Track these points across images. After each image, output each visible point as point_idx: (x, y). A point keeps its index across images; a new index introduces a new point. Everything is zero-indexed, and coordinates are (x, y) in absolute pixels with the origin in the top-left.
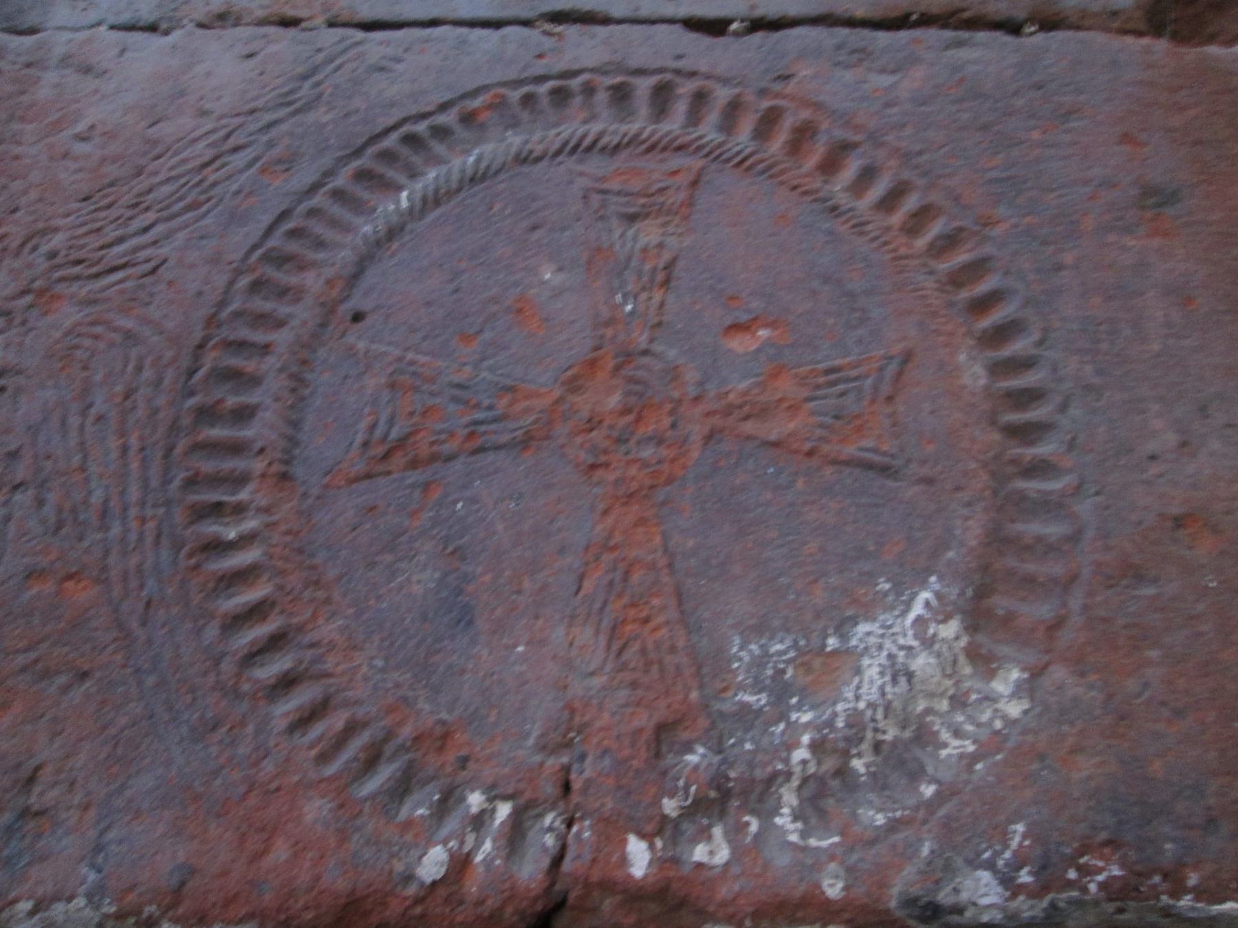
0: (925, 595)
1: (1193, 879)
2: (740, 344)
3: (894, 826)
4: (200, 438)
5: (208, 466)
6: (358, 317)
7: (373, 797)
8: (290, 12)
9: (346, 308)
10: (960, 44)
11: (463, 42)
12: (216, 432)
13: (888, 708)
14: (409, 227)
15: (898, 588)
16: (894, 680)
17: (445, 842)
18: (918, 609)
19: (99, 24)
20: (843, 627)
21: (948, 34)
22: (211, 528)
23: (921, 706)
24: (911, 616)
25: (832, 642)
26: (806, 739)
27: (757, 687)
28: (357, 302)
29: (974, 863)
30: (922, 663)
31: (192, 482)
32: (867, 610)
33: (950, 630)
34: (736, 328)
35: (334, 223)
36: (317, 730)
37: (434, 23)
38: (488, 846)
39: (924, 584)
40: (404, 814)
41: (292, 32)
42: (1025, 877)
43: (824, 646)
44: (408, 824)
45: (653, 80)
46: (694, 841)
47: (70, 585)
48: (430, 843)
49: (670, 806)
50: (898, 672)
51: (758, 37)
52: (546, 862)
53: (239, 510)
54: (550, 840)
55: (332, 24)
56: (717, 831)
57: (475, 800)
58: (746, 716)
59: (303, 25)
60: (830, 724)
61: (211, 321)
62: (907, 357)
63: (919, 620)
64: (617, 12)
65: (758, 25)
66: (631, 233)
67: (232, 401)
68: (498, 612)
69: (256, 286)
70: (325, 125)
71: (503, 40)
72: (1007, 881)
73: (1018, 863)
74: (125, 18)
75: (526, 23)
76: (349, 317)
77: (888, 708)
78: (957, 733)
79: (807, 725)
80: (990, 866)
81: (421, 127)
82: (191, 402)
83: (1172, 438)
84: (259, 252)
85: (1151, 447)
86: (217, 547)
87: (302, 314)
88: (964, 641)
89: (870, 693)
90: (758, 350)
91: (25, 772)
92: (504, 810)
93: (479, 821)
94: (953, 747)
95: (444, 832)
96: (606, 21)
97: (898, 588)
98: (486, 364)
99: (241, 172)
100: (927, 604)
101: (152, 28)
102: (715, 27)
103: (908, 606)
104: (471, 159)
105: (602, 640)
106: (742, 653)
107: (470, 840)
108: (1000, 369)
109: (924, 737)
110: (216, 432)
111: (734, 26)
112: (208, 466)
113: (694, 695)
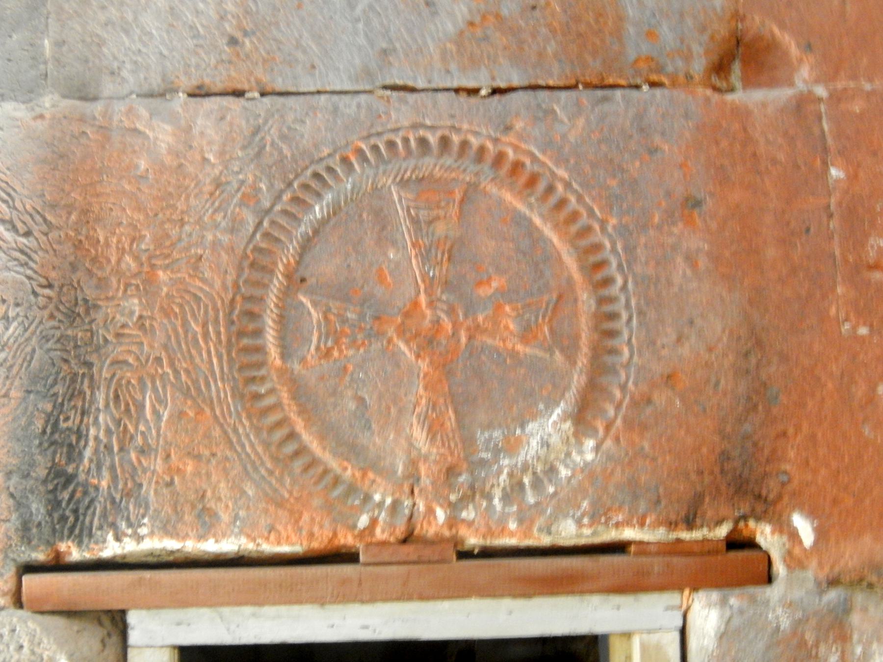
0: (558, 411)
1: (648, 521)
2: (484, 292)
3: (537, 504)
4: (241, 346)
5: (247, 359)
6: (303, 280)
7: (338, 497)
8: (239, 86)
9: (297, 277)
10: (605, 99)
11: (336, 109)
12: (245, 341)
13: (539, 458)
14: (321, 230)
15: (547, 407)
16: (542, 447)
17: (368, 513)
18: (554, 417)
19: (131, 93)
20: (523, 426)
21: (600, 93)
22: (254, 388)
23: (552, 456)
24: (551, 421)
25: (518, 432)
26: (505, 471)
27: (487, 450)
28: (302, 272)
29: (566, 516)
30: (555, 440)
31: (241, 369)
32: (534, 417)
33: (568, 425)
34: (479, 284)
35: (282, 228)
36: (312, 472)
37: (319, 92)
38: (383, 514)
39: (558, 405)
40: (349, 502)
41: (241, 101)
42: (586, 521)
43: (515, 433)
44: (352, 507)
45: (439, 134)
46: (461, 510)
47: (198, 417)
48: (361, 514)
49: (453, 498)
50: (545, 444)
51: (497, 97)
52: (405, 519)
53: (263, 379)
54: (407, 512)
55: (263, 94)
56: (471, 507)
57: (377, 497)
58: (483, 463)
59: (248, 95)
60: (516, 465)
61: (236, 285)
62: (560, 297)
63: (555, 423)
64: (421, 84)
65: (496, 91)
66: (431, 229)
67: (251, 327)
68: (381, 422)
69: (252, 265)
70: (270, 167)
71: (359, 106)
72: (579, 523)
73: (583, 515)
74: (146, 88)
75: (370, 92)
76: (299, 280)
77: (539, 458)
78: (567, 466)
79: (506, 466)
80: (573, 516)
81: (321, 169)
82: (234, 329)
83: (674, 337)
84: (251, 246)
85: (665, 340)
86: (257, 397)
87: (278, 281)
88: (572, 430)
89: (532, 452)
90: (491, 296)
91: (201, 493)
92: (389, 501)
93: (381, 505)
94: (564, 472)
95: (366, 509)
96: (413, 90)
97: (547, 407)
98: (368, 304)
99: (233, 196)
100: (558, 415)
101: (162, 95)
102: (473, 92)
103: (551, 416)
104: (349, 186)
105: (425, 434)
106: (481, 437)
107: (376, 513)
108: (602, 301)
109: (552, 470)
110: (245, 341)
111: (483, 92)
112: (247, 359)
113: (462, 455)
